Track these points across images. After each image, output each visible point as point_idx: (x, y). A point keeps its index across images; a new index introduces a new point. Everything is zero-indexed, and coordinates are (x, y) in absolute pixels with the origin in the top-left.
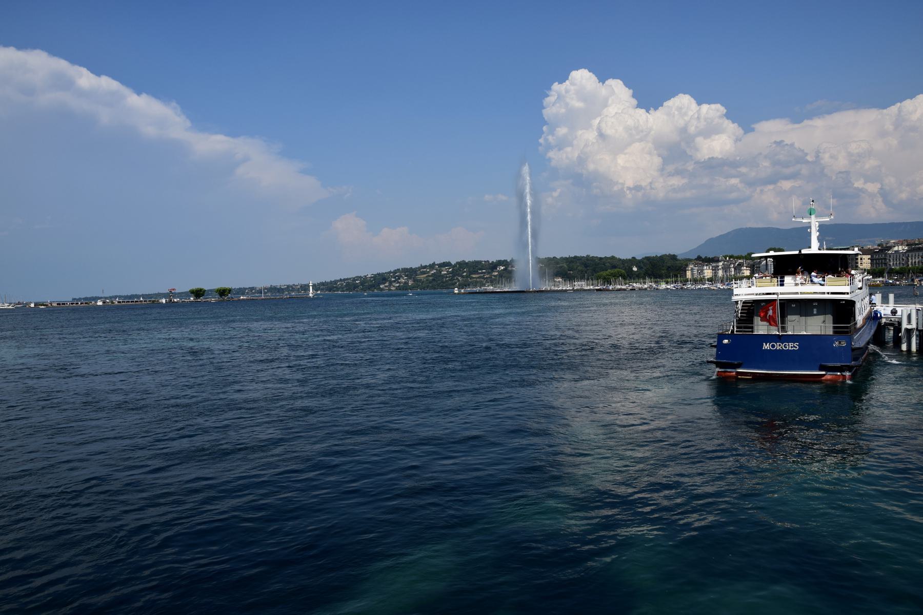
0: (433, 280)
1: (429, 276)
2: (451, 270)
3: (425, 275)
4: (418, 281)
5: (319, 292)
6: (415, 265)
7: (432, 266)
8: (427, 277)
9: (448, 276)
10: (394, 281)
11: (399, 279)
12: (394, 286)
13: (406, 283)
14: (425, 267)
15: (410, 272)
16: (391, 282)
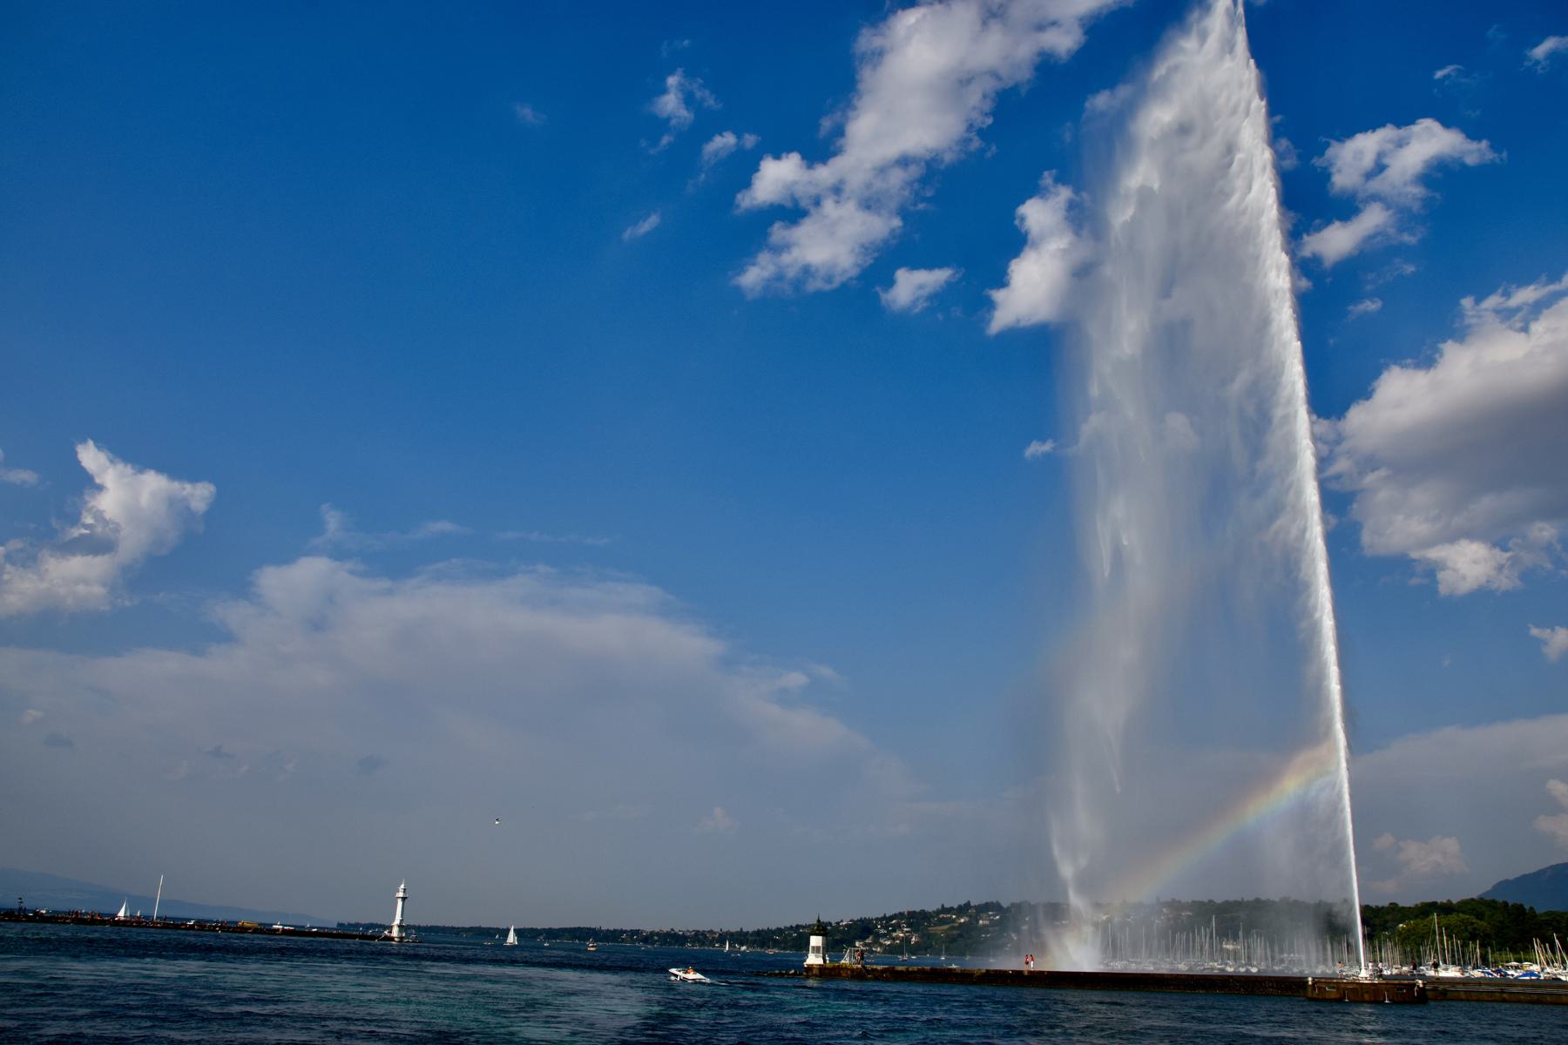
0: (960, 935)
1: (953, 928)
2: (998, 917)
3: (946, 927)
4: (929, 936)
5: (744, 948)
6: (931, 907)
7: (963, 910)
8: (948, 929)
9: (990, 929)
10: (884, 936)
11: (894, 931)
12: (881, 945)
13: (907, 940)
14: (950, 910)
15: (917, 920)
16: (878, 936)
